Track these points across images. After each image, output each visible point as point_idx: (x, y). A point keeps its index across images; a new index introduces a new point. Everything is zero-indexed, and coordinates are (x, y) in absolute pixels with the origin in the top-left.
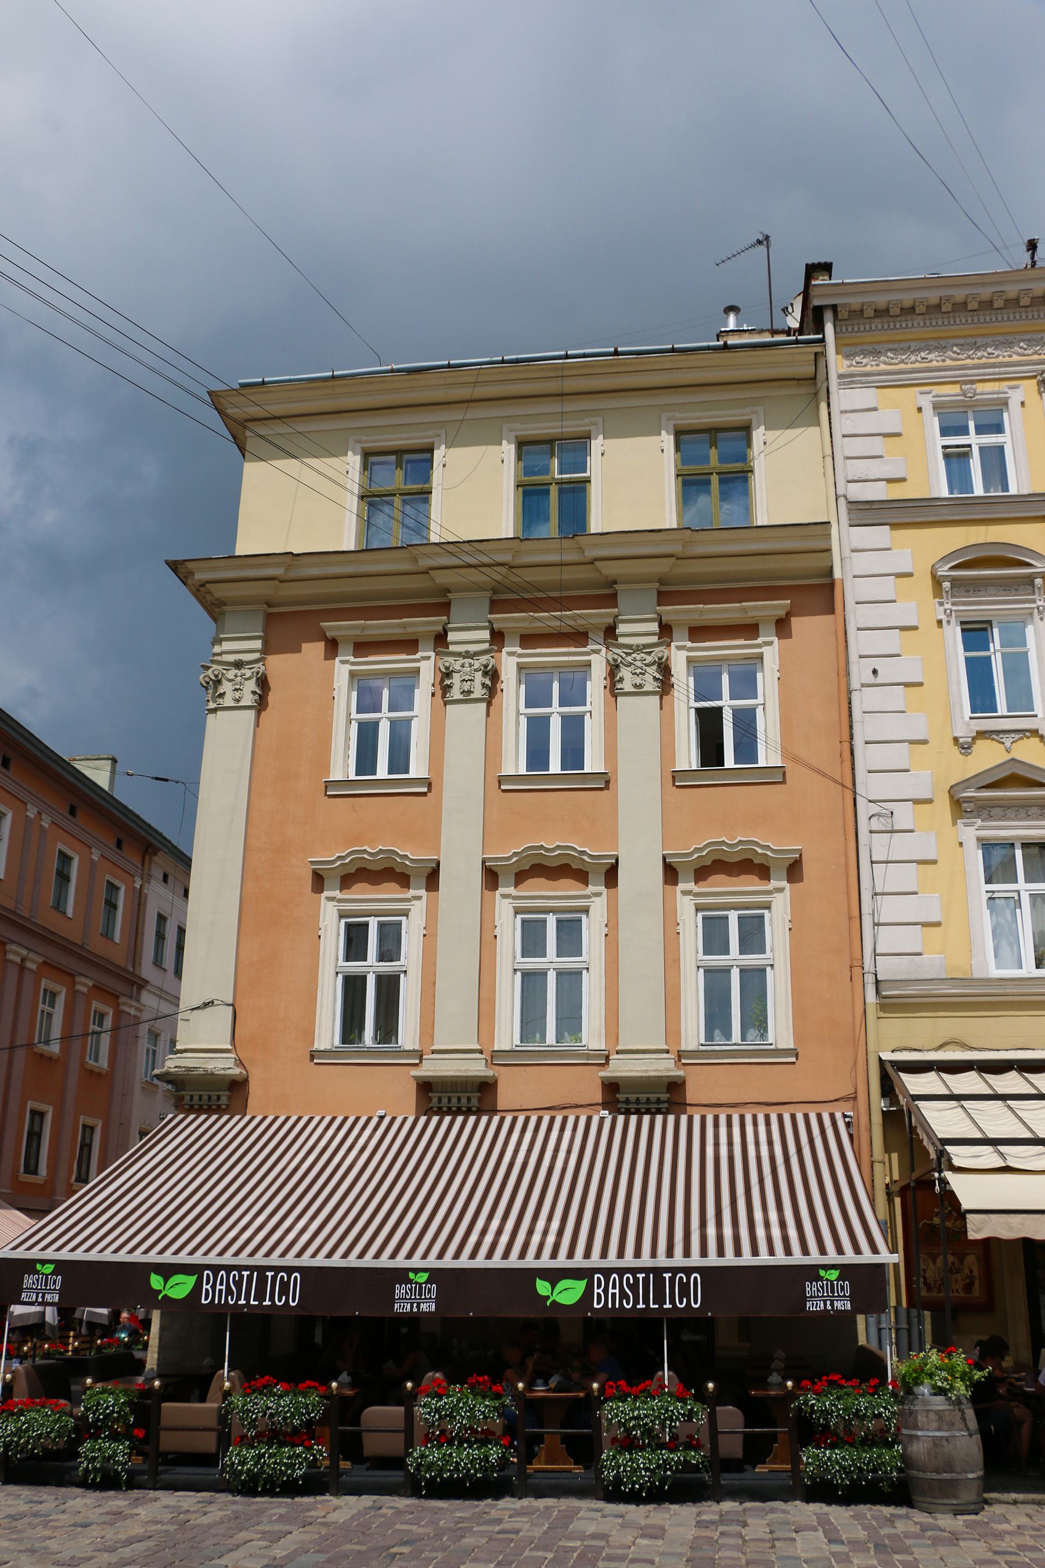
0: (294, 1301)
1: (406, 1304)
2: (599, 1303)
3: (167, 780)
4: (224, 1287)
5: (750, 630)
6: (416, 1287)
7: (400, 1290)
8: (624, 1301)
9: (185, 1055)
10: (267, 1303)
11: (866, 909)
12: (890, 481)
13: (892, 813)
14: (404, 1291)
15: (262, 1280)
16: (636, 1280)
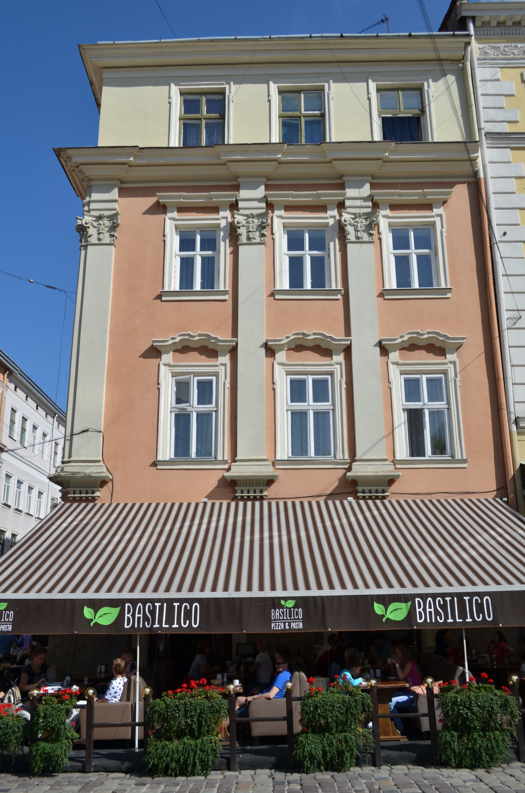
0: (195, 624)
1: (280, 623)
2: (421, 619)
3: (55, 288)
4: (141, 615)
5: (429, 207)
6: (286, 611)
7: (276, 614)
8: (438, 617)
9: (69, 464)
10: (175, 626)
11: (509, 374)
12: (509, 122)
13: (520, 317)
14: (278, 614)
15: (171, 609)
16: (445, 602)
